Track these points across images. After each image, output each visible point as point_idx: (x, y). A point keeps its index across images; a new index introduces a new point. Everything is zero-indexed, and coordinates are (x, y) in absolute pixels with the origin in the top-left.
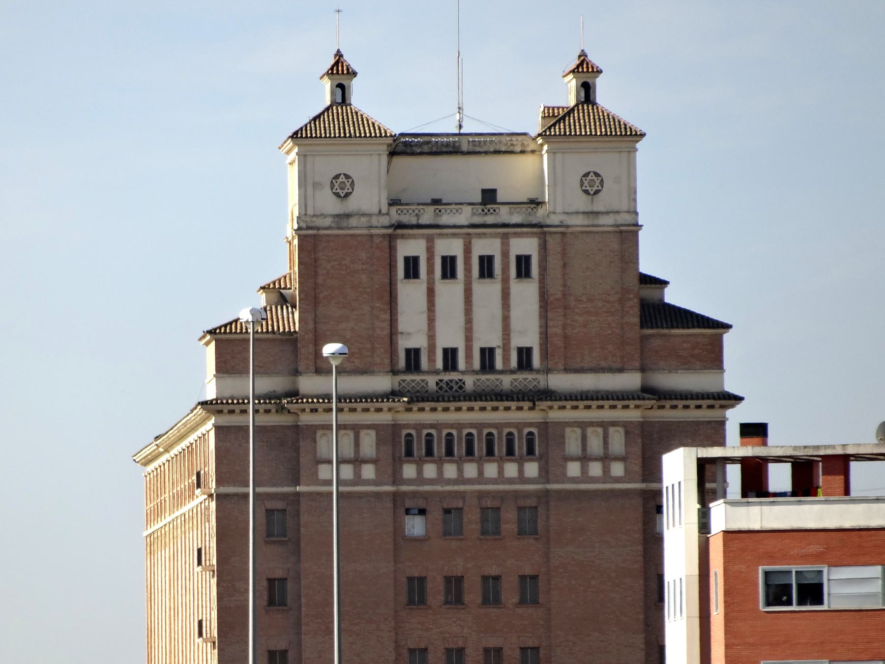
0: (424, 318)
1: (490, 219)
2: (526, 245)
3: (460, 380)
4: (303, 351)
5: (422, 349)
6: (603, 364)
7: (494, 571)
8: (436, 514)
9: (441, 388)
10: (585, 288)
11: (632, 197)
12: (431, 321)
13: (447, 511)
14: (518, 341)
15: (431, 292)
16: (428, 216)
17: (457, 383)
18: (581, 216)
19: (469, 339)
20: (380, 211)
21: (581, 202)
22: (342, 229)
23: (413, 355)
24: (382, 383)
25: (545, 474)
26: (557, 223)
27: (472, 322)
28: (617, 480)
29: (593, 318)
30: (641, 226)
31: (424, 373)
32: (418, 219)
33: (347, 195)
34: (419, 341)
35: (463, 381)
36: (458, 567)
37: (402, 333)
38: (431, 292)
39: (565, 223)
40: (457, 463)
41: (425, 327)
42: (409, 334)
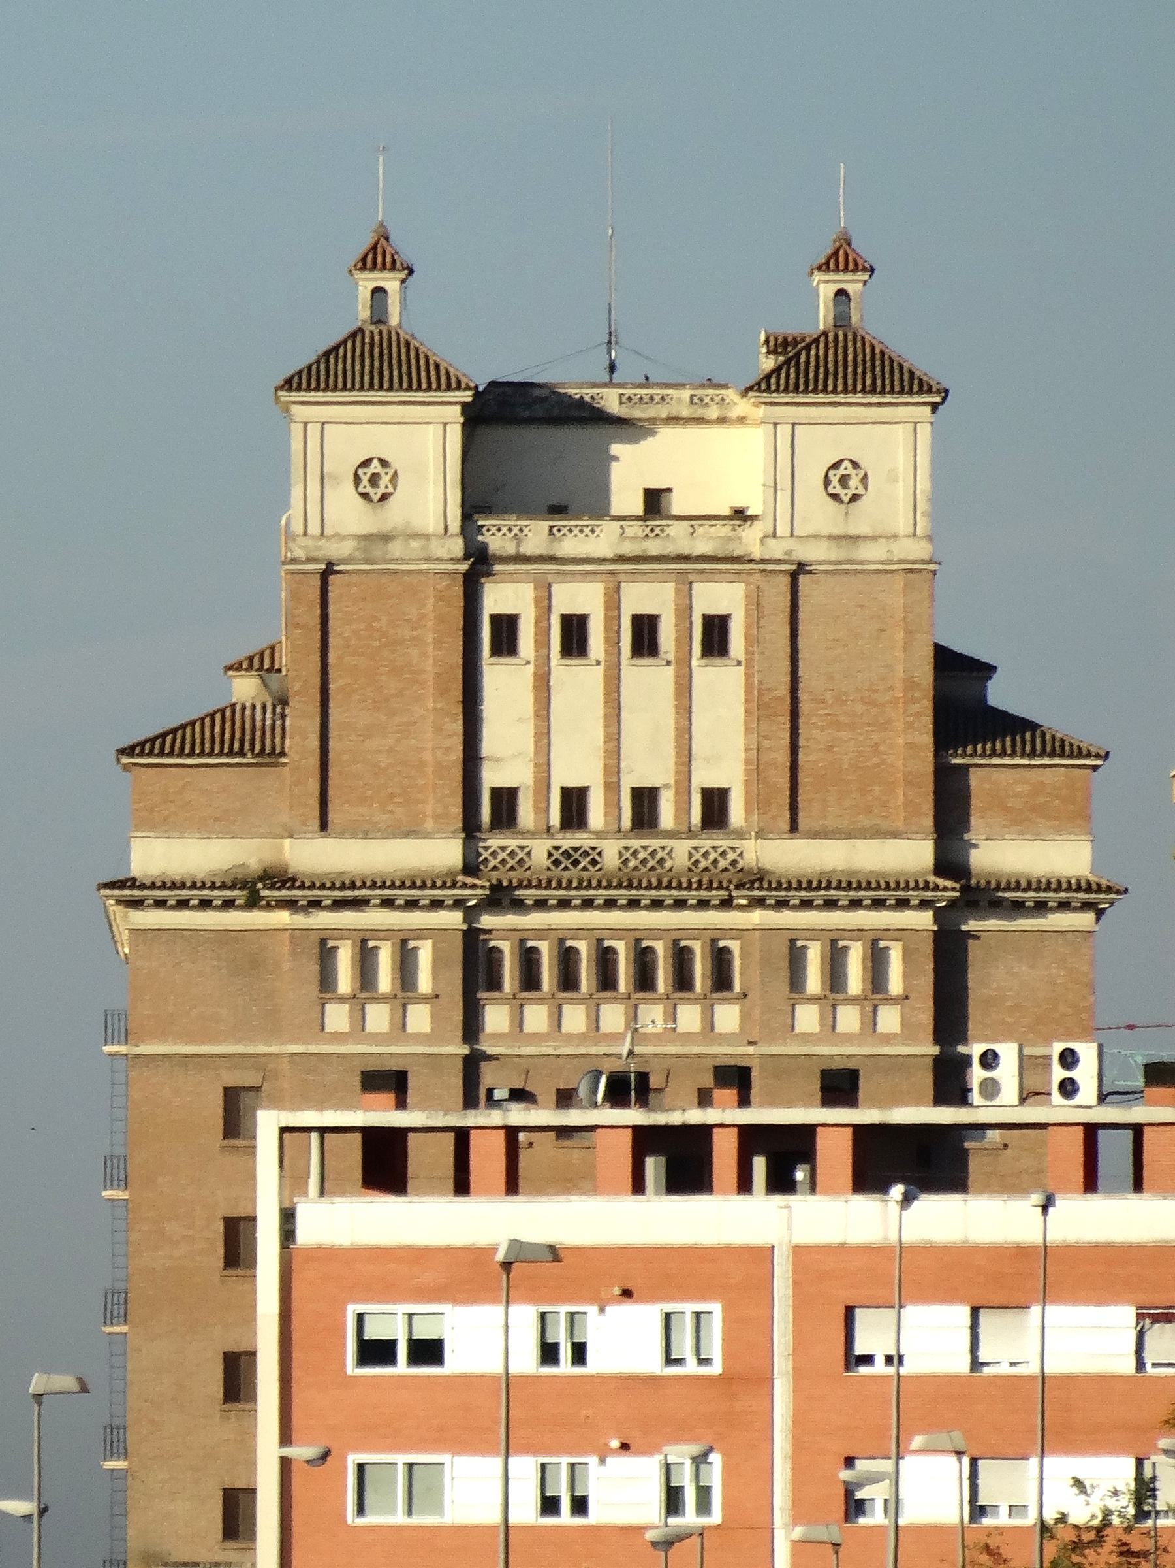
0: (527, 731)
6: (865, 821)
9: (556, 863)
10: (831, 678)
14: (705, 777)
15: (543, 684)
18: (824, 544)
26: (779, 555)
28: (888, 1039)
29: (844, 735)
32: (518, 546)
35: (598, 851)
38: (543, 684)
42: (498, 760)
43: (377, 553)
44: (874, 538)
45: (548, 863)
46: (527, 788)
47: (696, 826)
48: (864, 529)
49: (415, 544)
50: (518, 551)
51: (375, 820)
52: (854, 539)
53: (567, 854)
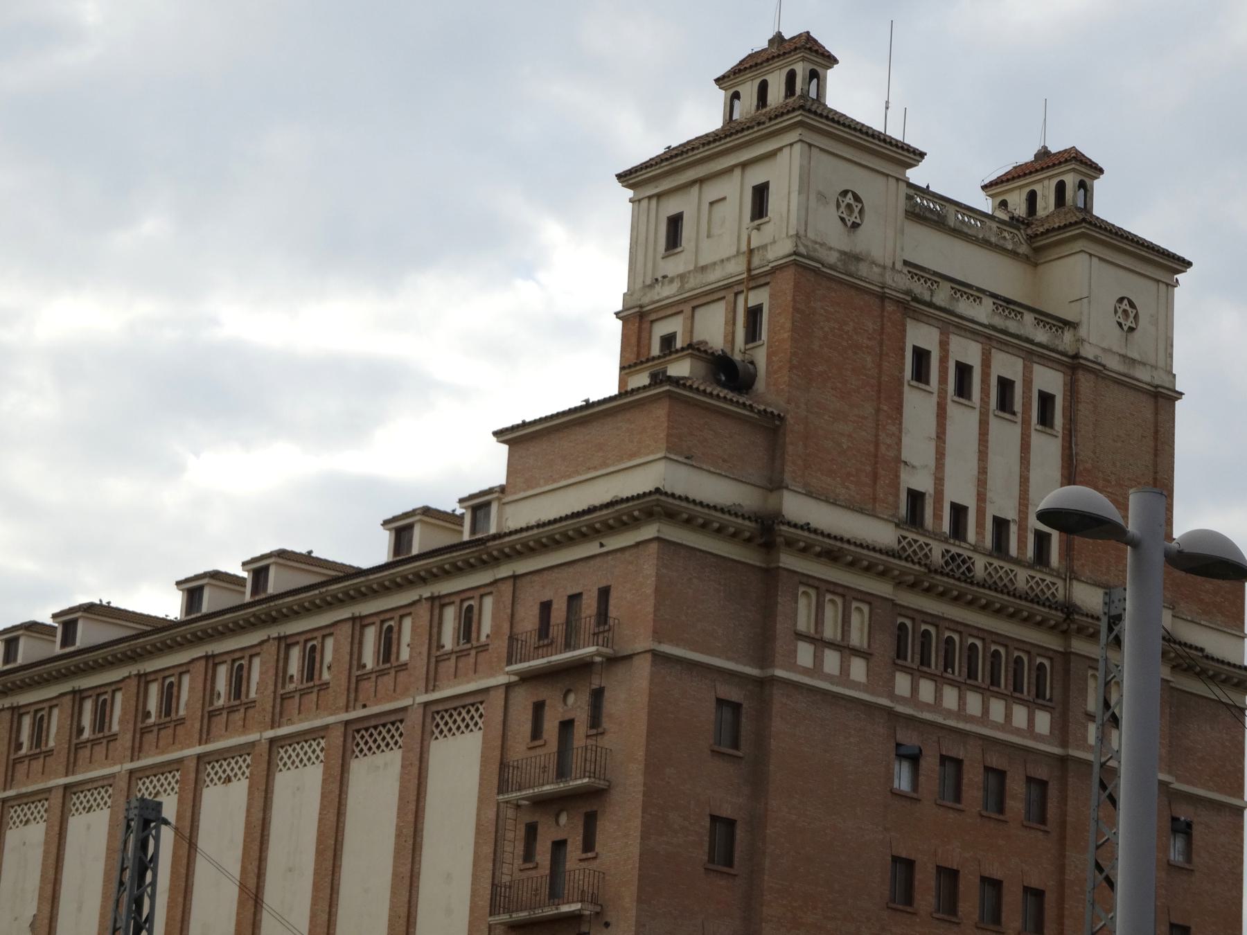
0: (931, 448)
1: (1012, 326)
2: (1050, 380)
3: (970, 558)
4: (790, 449)
5: (927, 496)
7: (997, 874)
8: (929, 763)
11: (1169, 351)
12: (940, 455)
13: (944, 759)
16: (942, 296)
17: (964, 562)
18: (1117, 358)
19: (981, 498)
20: (894, 263)
21: (1114, 338)
22: (851, 275)
23: (916, 498)
24: (882, 533)
25: (1062, 730)
26: (1091, 357)
27: (986, 473)
30: (1182, 394)
31: (925, 533)
32: (931, 296)
33: (855, 226)
34: (922, 482)
35: (972, 561)
36: (954, 856)
37: (906, 463)
39: (1099, 360)
40: (959, 688)
41: (932, 463)
42: (914, 467)
43: (853, 268)
44: (1144, 364)
45: (941, 562)
46: (930, 495)
47: (1030, 558)
48: (1136, 356)
49: (876, 269)
50: (931, 300)
51: (837, 491)
52: (1133, 361)
53: (953, 558)
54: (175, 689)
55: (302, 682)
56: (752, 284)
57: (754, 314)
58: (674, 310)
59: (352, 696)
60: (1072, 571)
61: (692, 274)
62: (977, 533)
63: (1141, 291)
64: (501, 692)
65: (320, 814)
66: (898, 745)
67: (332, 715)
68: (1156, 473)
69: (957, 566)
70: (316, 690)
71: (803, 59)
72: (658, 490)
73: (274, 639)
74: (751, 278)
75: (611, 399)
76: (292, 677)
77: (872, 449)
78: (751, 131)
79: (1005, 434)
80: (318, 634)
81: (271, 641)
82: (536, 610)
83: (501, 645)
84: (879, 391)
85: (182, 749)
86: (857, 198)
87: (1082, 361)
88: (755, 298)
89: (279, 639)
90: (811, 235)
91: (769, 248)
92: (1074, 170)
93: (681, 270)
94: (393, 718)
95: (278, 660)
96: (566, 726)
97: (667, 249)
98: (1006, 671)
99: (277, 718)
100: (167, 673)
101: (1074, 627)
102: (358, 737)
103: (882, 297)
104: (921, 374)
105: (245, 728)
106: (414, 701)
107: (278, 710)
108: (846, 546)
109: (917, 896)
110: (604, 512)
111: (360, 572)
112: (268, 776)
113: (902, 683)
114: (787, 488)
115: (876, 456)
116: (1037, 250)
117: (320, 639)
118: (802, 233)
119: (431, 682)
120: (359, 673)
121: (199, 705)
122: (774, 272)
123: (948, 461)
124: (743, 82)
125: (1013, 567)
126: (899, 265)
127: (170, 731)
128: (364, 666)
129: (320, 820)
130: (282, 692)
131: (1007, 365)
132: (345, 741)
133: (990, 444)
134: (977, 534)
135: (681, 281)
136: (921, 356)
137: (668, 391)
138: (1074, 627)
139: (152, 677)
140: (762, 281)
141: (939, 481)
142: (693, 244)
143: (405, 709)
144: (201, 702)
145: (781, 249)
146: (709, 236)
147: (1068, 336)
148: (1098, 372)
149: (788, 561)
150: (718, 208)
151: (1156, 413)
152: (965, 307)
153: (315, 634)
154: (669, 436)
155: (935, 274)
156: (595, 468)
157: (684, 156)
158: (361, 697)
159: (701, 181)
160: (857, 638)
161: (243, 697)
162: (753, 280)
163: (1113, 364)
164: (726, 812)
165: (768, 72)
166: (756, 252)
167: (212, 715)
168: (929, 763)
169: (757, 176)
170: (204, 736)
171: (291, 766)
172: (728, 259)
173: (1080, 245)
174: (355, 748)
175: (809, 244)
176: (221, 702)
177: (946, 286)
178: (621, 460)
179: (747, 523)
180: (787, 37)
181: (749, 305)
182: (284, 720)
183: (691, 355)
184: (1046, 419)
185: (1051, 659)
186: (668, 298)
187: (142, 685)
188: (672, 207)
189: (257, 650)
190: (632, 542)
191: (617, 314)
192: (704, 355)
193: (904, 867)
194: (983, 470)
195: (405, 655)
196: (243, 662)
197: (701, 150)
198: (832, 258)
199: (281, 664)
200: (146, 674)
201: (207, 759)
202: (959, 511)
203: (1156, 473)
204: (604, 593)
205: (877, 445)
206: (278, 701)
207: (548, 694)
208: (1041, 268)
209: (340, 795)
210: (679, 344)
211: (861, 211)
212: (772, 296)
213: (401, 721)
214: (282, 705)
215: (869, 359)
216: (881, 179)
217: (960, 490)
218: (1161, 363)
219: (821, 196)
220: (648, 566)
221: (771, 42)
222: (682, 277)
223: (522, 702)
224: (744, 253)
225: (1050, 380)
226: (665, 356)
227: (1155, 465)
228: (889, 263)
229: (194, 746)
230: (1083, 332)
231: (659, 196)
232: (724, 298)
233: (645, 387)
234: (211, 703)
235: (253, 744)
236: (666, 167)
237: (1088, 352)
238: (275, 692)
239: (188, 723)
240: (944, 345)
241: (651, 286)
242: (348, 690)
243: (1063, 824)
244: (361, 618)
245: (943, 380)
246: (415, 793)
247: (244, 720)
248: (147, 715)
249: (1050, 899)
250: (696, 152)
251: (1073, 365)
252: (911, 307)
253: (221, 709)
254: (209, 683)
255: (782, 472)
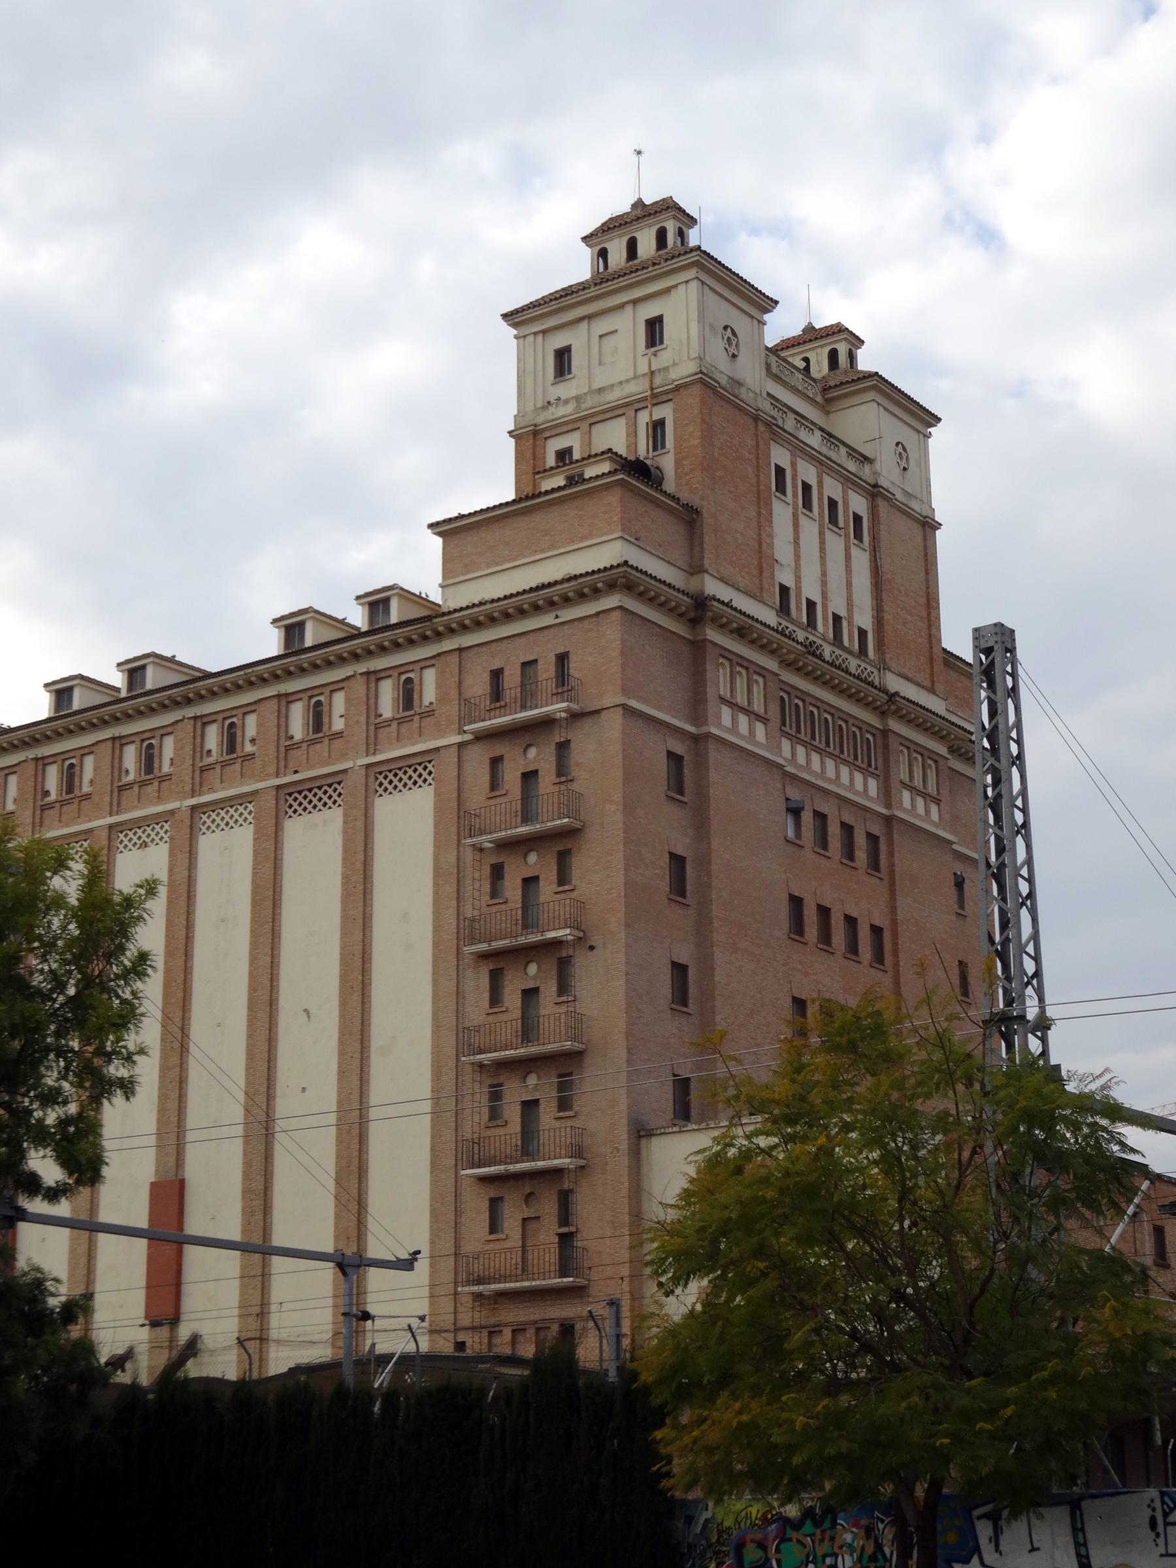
0: (791, 548)
4: (707, 539)
12: (797, 557)
23: (784, 590)
24: (769, 617)
25: (887, 795)
31: (792, 621)
33: (734, 356)
34: (786, 577)
41: (793, 564)
43: (737, 391)
54: (77, 769)
55: (222, 755)
56: (654, 401)
57: (658, 427)
58: (570, 427)
59: (282, 764)
60: (885, 663)
61: (588, 397)
62: (824, 625)
63: (909, 438)
64: (454, 752)
65: (254, 869)
66: (787, 799)
67: (261, 781)
68: (928, 588)
69: (812, 650)
70: (239, 760)
71: (675, 217)
72: (626, 563)
73: (189, 718)
74: (654, 396)
75: (507, 504)
76: (209, 751)
77: (756, 545)
78: (645, 271)
79: (835, 544)
80: (240, 712)
81: (186, 720)
82: (486, 677)
83: (453, 709)
84: (759, 498)
85: (90, 821)
86: (734, 334)
87: (881, 489)
88: (659, 413)
89: (195, 718)
90: (708, 359)
91: (671, 369)
92: (845, 339)
93: (574, 393)
94: (330, 781)
95: (194, 737)
96: (529, 777)
97: (555, 378)
98: (848, 743)
99: (197, 788)
100: (66, 756)
101: (893, 707)
102: (290, 800)
103: (756, 419)
104: (781, 487)
105: (160, 799)
106: (354, 763)
107: (197, 780)
108: (755, 624)
109: (807, 929)
110: (566, 585)
111: (209, 675)
112: (191, 839)
113: (786, 745)
114: (707, 572)
115: (760, 552)
116: (828, 401)
117: (240, 716)
118: (702, 356)
119: (372, 746)
120: (288, 743)
121: (108, 781)
122: (678, 390)
123: (803, 562)
124: (612, 239)
125: (848, 656)
126: (765, 395)
127: (75, 806)
128: (292, 737)
129: (255, 874)
130: (201, 765)
131: (832, 488)
132: (277, 804)
133: (827, 552)
134: (824, 626)
135: (577, 402)
136: (780, 471)
137: (622, 479)
138: (893, 707)
139: (51, 760)
140: (665, 398)
141: (798, 578)
142: (585, 371)
143: (345, 771)
144: (110, 778)
145: (685, 369)
146: (600, 364)
147: (867, 468)
148: (890, 499)
149: (712, 634)
150: (610, 342)
151: (925, 540)
152: (803, 435)
153: (234, 712)
154: (622, 518)
155: (785, 405)
156: (543, 551)
157: (575, 295)
158: (291, 765)
159: (589, 317)
160: (758, 706)
161: (156, 771)
162: (656, 398)
163: (899, 496)
164: (680, 851)
165: (637, 230)
166: (657, 373)
167: (121, 789)
168: (807, 817)
169: (650, 311)
170: (115, 808)
171: (234, 825)
172: (627, 381)
173: (871, 395)
174: (288, 810)
175: (709, 366)
176: (131, 777)
177: (791, 416)
178: (572, 542)
179: (685, 598)
180: (647, 203)
181: (654, 418)
182: (205, 789)
183: (610, 459)
184: (858, 535)
185: (873, 735)
186: (565, 416)
187: (40, 767)
188: (559, 341)
189: (170, 730)
190: (593, 612)
191: (510, 432)
192: (619, 459)
193: (796, 902)
194: (824, 574)
195: (338, 724)
196: (153, 741)
197: (593, 289)
198: (724, 380)
199: (198, 740)
200: (43, 758)
201: (119, 828)
202: (811, 605)
203: (928, 588)
204: (562, 659)
205: (760, 544)
206: (198, 772)
207: (500, 749)
208: (832, 416)
209: (275, 851)
210: (576, 455)
211: (737, 345)
212: (675, 410)
213: (339, 783)
214: (201, 777)
215: (750, 469)
216: (748, 320)
217: (811, 590)
218: (925, 500)
219: (712, 328)
220: (612, 633)
221: (634, 206)
222: (578, 399)
223: (478, 762)
224: (644, 375)
225: (859, 504)
226: (558, 467)
227: (927, 581)
228: (758, 392)
229: (105, 818)
230: (877, 466)
231: (544, 332)
232: (624, 414)
233: (560, 489)
234: (120, 779)
235: (172, 812)
236: (554, 305)
237: (883, 482)
238: (193, 765)
239: (95, 798)
240: (793, 464)
241: (544, 408)
242: (278, 758)
243: (892, 873)
244: (287, 695)
245: (795, 495)
246: (363, 844)
247: (159, 791)
248: (47, 793)
249: (887, 935)
250: (587, 291)
251: (875, 492)
252: (775, 432)
253: (130, 785)
254: (116, 761)
255: (702, 558)
